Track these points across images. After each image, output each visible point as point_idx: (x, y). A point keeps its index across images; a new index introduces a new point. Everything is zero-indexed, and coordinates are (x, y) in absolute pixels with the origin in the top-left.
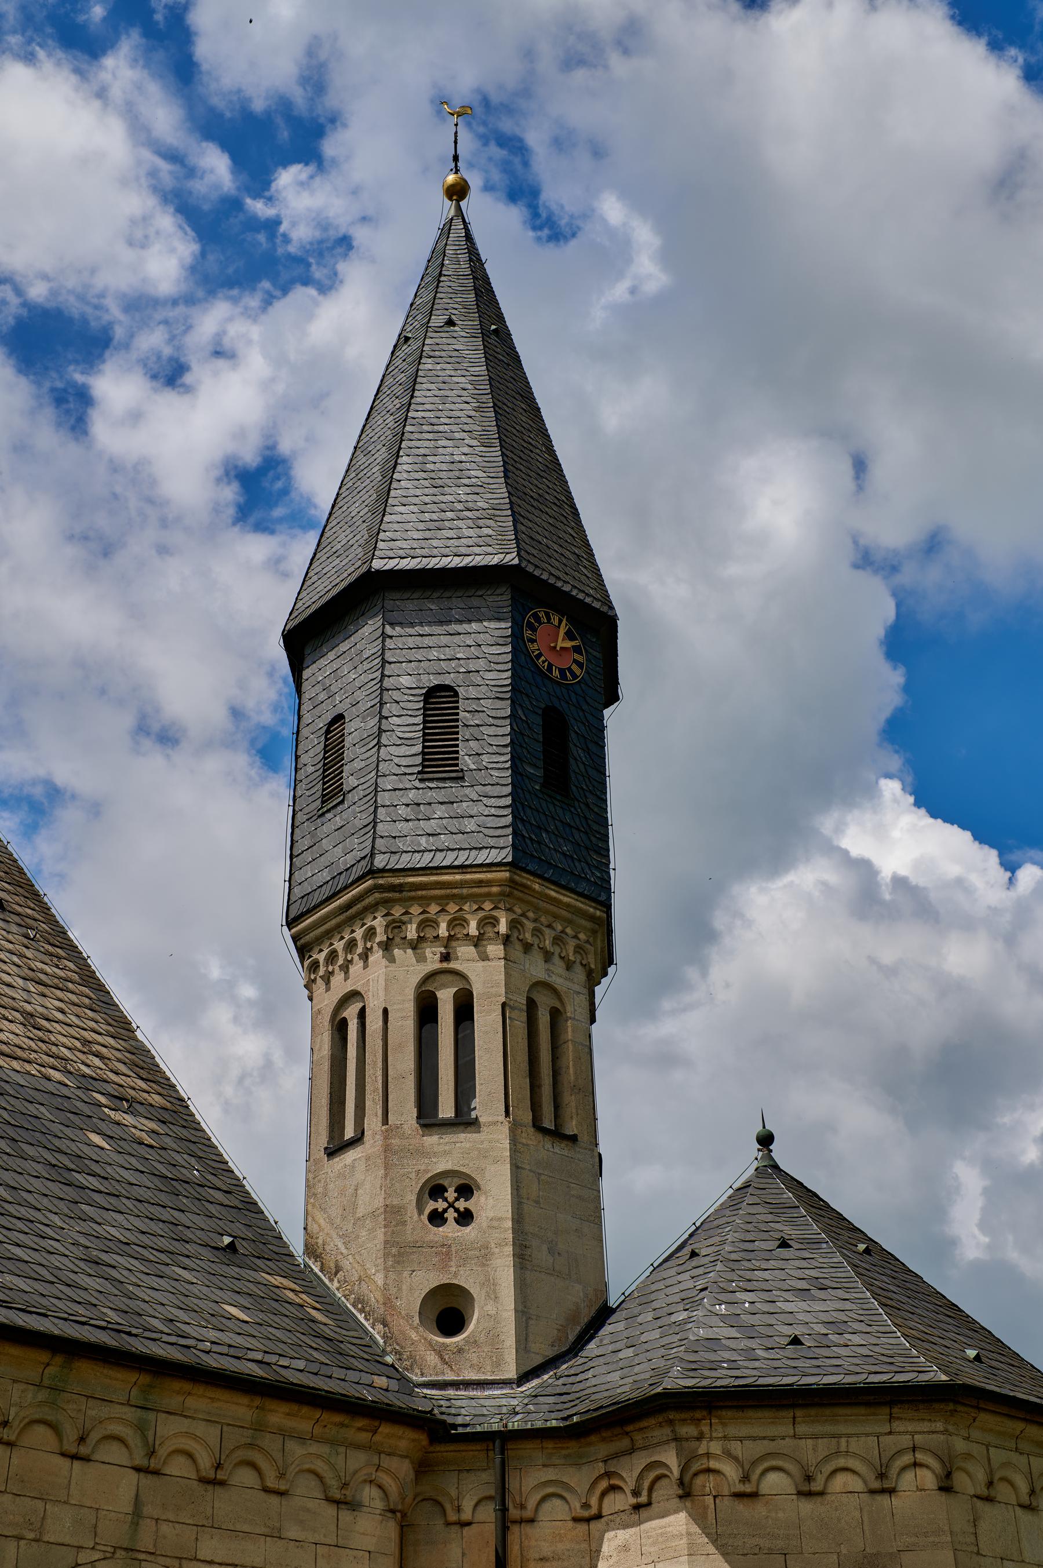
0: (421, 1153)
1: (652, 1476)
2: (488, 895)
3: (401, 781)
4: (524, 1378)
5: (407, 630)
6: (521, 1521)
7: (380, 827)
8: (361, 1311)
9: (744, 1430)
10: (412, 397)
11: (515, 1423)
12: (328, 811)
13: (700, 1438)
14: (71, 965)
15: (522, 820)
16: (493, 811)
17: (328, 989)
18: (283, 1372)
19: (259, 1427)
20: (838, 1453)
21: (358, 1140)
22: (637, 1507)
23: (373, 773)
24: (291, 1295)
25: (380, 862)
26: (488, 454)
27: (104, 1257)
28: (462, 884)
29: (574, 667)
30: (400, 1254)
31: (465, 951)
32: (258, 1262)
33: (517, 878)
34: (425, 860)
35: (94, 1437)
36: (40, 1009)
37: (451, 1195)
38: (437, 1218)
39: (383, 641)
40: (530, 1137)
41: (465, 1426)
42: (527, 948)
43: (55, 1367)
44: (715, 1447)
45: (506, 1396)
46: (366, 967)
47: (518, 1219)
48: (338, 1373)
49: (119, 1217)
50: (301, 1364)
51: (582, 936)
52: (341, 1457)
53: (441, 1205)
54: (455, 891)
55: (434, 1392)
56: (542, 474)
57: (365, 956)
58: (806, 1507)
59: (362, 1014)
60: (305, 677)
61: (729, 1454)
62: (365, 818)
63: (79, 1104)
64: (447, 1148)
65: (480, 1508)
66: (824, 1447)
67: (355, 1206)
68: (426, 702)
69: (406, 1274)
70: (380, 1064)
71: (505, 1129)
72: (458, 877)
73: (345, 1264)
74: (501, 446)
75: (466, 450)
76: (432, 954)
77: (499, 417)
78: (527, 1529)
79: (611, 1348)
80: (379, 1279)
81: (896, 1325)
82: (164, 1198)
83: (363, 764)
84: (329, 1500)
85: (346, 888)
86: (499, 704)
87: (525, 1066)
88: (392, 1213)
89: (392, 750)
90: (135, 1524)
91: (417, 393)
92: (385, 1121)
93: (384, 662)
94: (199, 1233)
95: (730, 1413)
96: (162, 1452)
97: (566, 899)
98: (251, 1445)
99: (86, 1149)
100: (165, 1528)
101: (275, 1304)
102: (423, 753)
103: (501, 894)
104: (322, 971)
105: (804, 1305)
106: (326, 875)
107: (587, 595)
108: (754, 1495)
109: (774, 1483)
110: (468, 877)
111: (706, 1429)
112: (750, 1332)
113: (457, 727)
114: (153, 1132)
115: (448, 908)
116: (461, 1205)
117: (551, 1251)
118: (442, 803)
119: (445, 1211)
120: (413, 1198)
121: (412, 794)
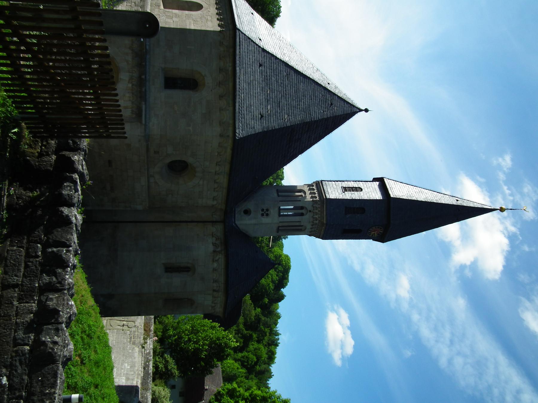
4: (236, 224)
21: (278, 196)
22: (213, 243)
37: (267, 212)
38: (263, 210)
42: (312, 225)
53: (265, 211)
61: (219, 258)
70: (291, 200)
92: (280, 201)
116: (265, 214)
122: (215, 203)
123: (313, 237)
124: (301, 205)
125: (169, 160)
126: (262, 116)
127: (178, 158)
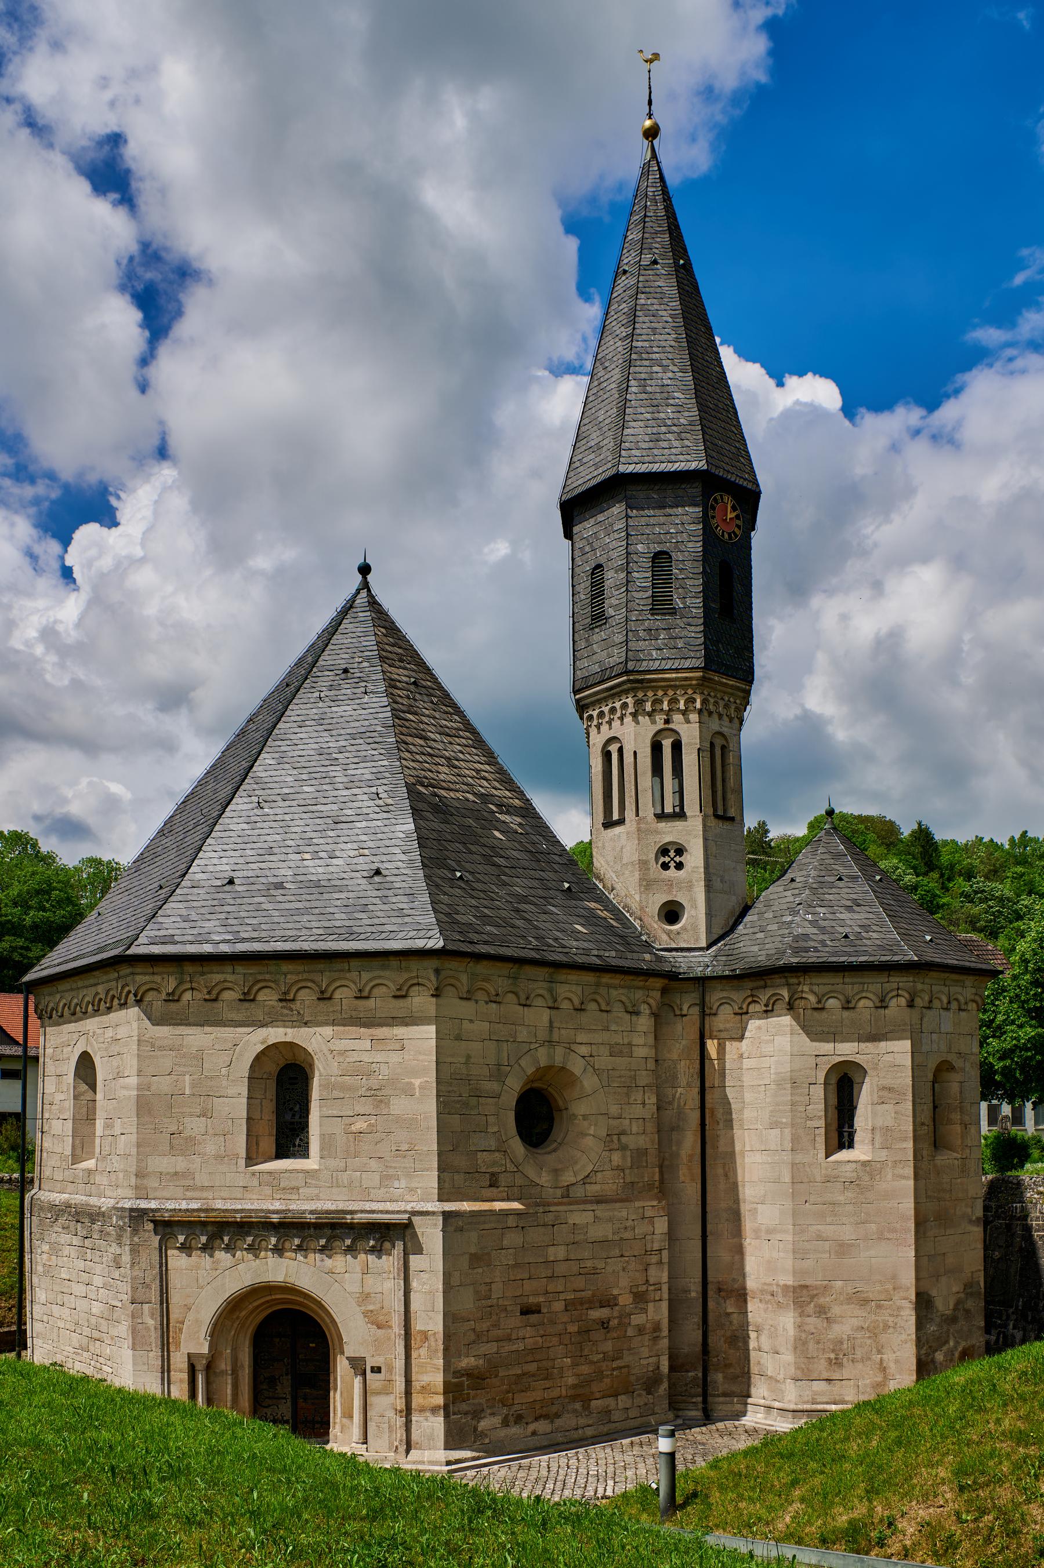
0: (657, 832)
1: (774, 998)
2: (690, 685)
3: (640, 615)
5: (641, 512)
6: (710, 1015)
7: (630, 644)
8: (628, 912)
9: (820, 981)
10: (634, 329)
11: (708, 972)
12: (596, 627)
13: (799, 984)
14: (456, 717)
15: (709, 639)
16: (693, 634)
17: (599, 732)
18: (608, 959)
19: (598, 985)
20: (863, 991)
21: (621, 822)
22: (766, 1011)
23: (624, 609)
24: (599, 912)
25: (631, 665)
26: (685, 379)
27: (519, 906)
28: (676, 679)
29: (736, 530)
30: (647, 885)
31: (677, 718)
32: (581, 895)
33: (706, 675)
35: (532, 996)
36: (452, 754)
37: (672, 854)
38: (665, 866)
39: (627, 520)
40: (712, 822)
41: (684, 973)
42: (710, 713)
43: (515, 969)
44: (806, 988)
45: (702, 956)
46: (622, 724)
47: (707, 867)
48: (629, 955)
49: (518, 880)
50: (613, 954)
51: (738, 701)
52: (632, 994)
53: (667, 859)
54: (672, 683)
55: (666, 953)
56: (716, 385)
57: (621, 718)
58: (846, 1014)
59: (620, 750)
60: (575, 532)
61: (812, 991)
62: (619, 638)
63: (485, 814)
64: (670, 829)
65: (691, 1009)
67: (621, 858)
68: (653, 562)
69: (651, 895)
70: (633, 783)
71: (700, 819)
72: (674, 675)
73: (618, 886)
74: (692, 371)
75: (670, 375)
76: (660, 719)
77: (682, 297)
79: (751, 930)
80: (637, 897)
81: (894, 927)
82: (534, 865)
83: (617, 602)
84: (627, 1012)
85: (611, 678)
86: (696, 564)
87: (709, 783)
88: (643, 864)
89: (635, 594)
90: (551, 1031)
91: (637, 325)
92: (637, 815)
93: (628, 534)
94: (553, 883)
95: (814, 974)
96: (559, 999)
97: (731, 683)
98: (594, 993)
99: (495, 842)
100: (563, 1032)
101: (594, 919)
102: (653, 596)
103: (697, 685)
104: (595, 722)
105: (849, 915)
106: (596, 668)
107: (745, 479)
108: (823, 1009)
109: (832, 1003)
110: (680, 675)
111: (802, 980)
112: (823, 930)
113: (671, 579)
114: (520, 824)
115: (668, 693)
116: (677, 859)
117: (721, 881)
118: (664, 629)
119: (669, 862)
120: (653, 856)
121: (646, 623)
122: (644, 1009)
123: (746, 714)
124: (648, 750)
125: (517, 1146)
126: (378, 872)
127: (512, 1115)
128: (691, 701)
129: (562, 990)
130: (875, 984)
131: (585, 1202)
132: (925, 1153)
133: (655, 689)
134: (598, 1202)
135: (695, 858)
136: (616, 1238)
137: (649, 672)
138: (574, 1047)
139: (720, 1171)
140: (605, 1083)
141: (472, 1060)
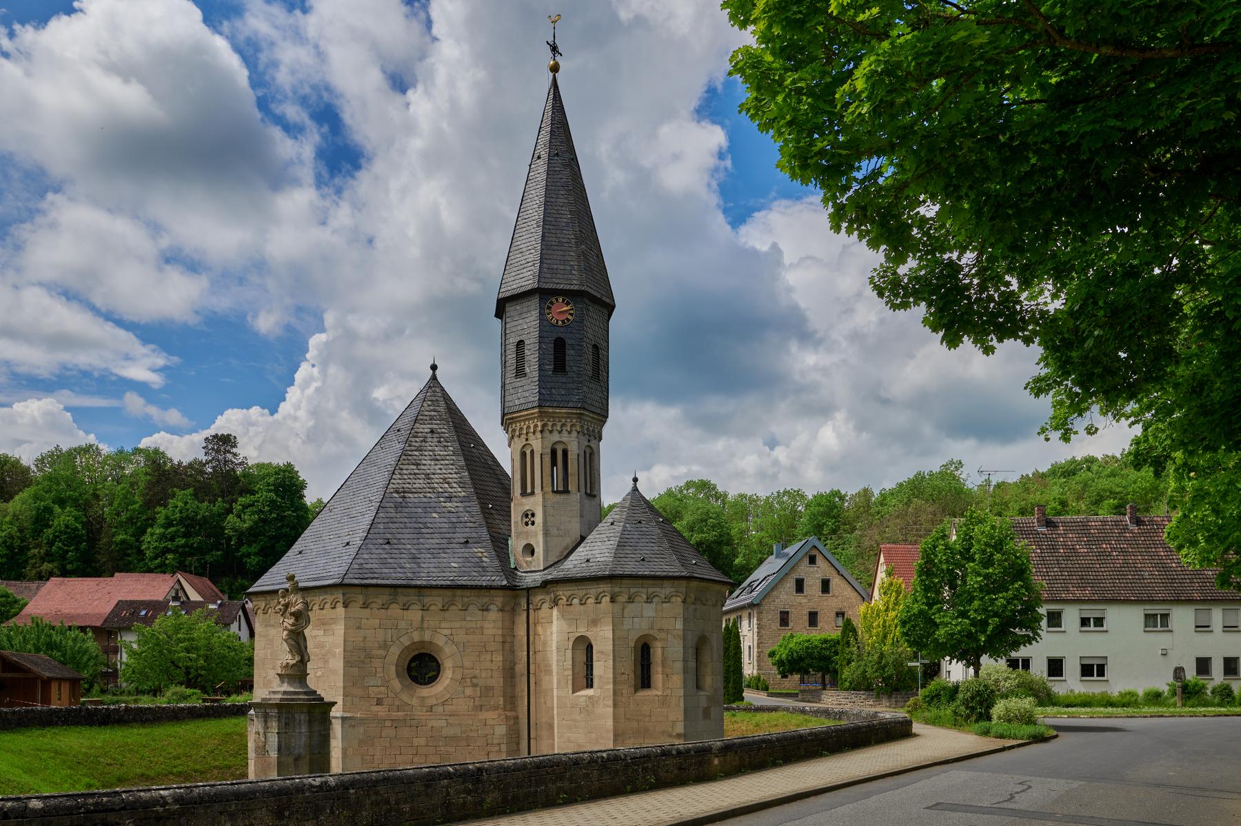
28: (527, 415)
34: (516, 409)
38: (527, 524)
40: (550, 496)
53: (527, 520)
66: (584, 592)
71: (541, 495)
72: (525, 413)
76: (523, 437)
78: (540, 611)
108: (571, 605)
116: (532, 519)
117: (558, 529)
120: (520, 519)
127: (393, 668)
128: (536, 426)
129: (427, 600)
130: (593, 590)
131: (440, 715)
132: (624, 692)
133: (520, 421)
134: (450, 715)
135: (539, 519)
136: (464, 735)
137: (518, 412)
138: (438, 630)
139: (542, 700)
140: (461, 649)
141: (368, 639)
